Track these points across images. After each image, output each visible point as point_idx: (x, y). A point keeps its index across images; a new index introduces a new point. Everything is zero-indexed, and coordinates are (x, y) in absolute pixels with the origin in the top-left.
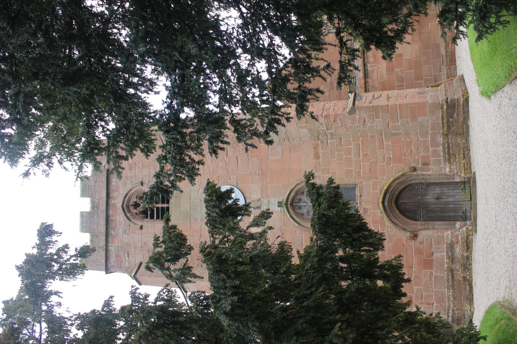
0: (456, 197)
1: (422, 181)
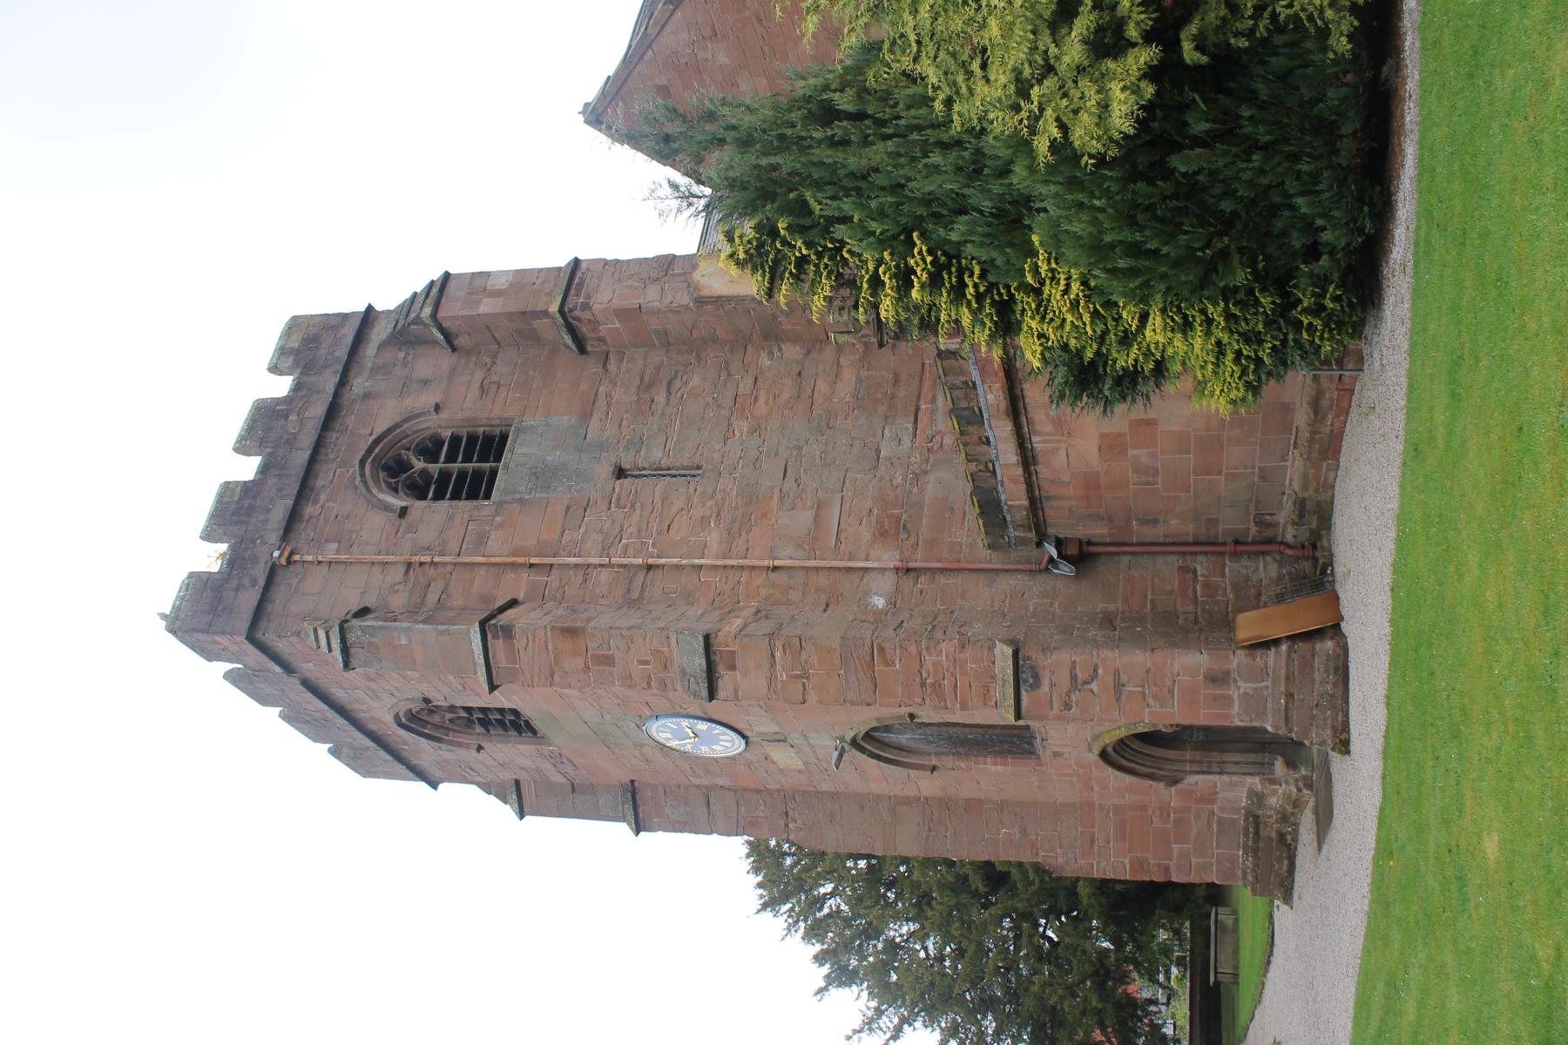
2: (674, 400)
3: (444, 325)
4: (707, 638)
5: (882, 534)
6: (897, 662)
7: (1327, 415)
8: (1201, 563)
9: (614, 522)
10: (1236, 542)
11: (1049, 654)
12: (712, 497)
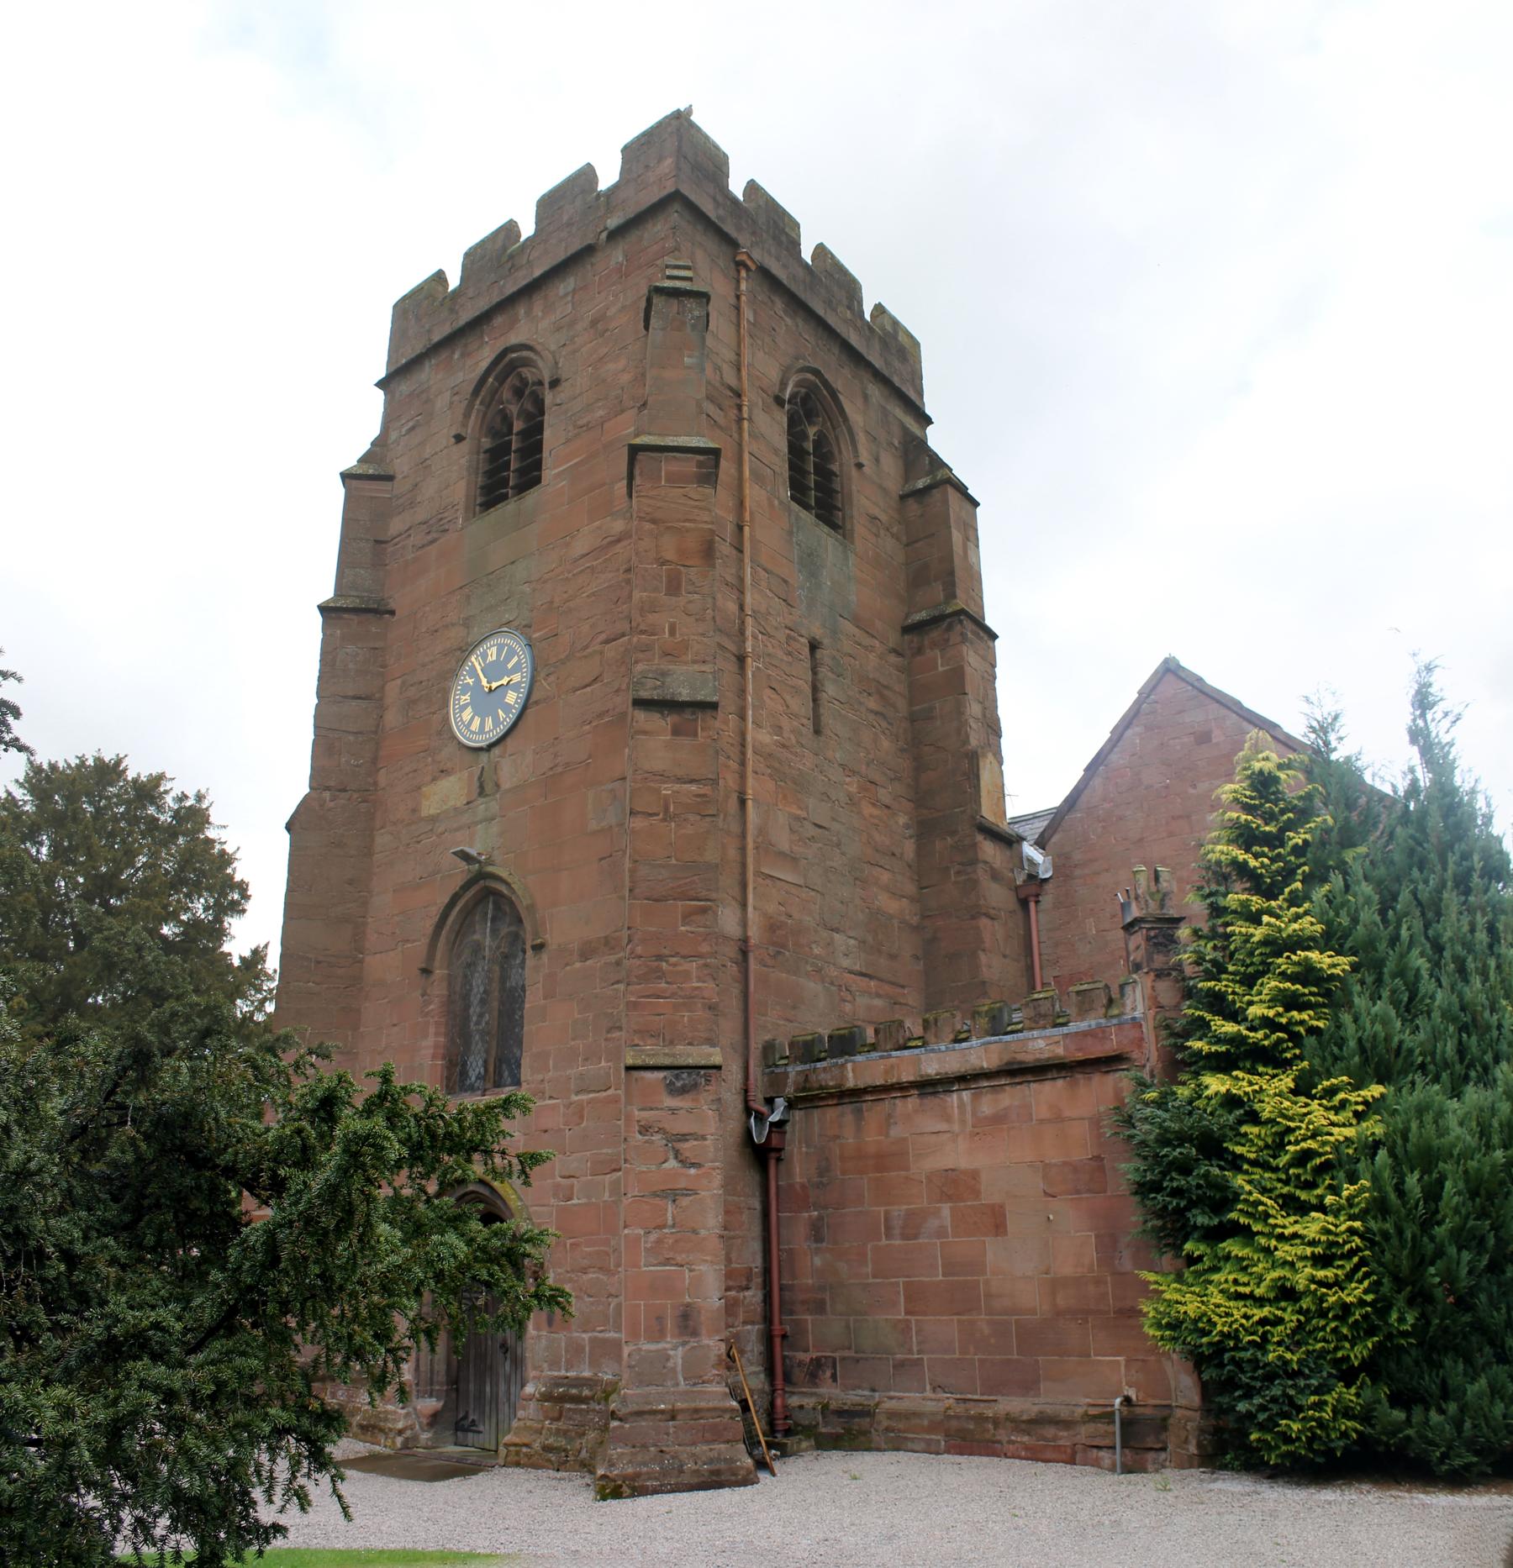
0: (507, 1405)
2: (871, 717)
3: (934, 491)
4: (713, 706)
5: (772, 927)
6: (688, 928)
7: (1029, 1434)
8: (753, 1296)
9: (776, 628)
10: (784, 1337)
11: (714, 1107)
12: (798, 742)
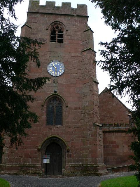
1: (63, 154)
